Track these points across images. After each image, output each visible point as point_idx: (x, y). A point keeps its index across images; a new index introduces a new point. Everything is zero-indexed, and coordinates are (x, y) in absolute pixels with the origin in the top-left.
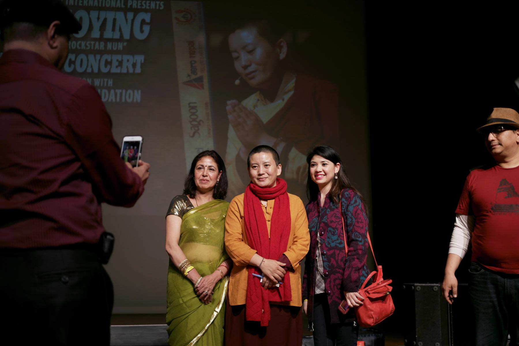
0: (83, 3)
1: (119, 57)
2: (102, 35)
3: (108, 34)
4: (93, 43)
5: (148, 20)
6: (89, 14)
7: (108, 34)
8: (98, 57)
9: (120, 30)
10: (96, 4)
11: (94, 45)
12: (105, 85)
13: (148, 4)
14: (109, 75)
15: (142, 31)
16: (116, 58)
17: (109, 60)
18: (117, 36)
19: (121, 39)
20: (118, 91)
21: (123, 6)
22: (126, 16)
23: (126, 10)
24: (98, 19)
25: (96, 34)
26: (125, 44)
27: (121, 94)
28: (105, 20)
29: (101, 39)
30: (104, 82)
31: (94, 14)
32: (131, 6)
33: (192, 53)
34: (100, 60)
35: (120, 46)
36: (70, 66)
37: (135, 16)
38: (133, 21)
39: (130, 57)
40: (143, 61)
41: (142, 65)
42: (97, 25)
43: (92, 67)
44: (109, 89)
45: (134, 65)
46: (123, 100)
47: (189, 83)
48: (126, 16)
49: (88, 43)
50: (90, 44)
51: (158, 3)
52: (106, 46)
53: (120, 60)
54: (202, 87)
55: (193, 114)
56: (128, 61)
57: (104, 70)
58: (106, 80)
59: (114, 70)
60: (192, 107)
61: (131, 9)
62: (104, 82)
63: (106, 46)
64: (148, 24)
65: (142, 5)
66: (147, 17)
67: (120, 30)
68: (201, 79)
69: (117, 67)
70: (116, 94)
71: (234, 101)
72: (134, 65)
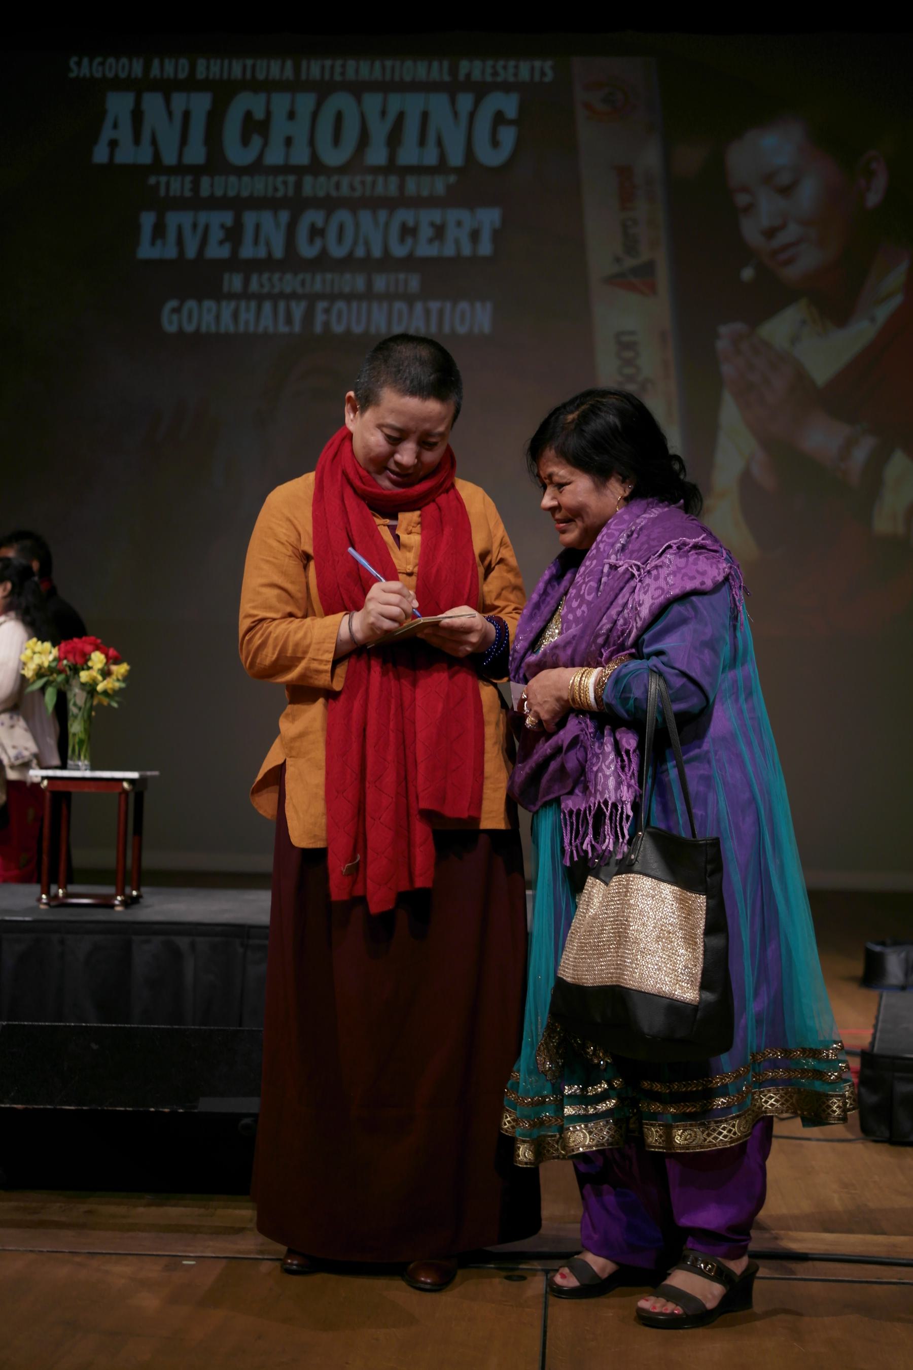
0: (343, 74)
1: (436, 215)
2: (392, 157)
3: (408, 155)
4: (369, 179)
5: (511, 112)
6: (359, 101)
7: (408, 155)
8: (383, 215)
9: (440, 143)
10: (377, 74)
11: (374, 183)
13: (511, 70)
14: (410, 263)
15: (495, 143)
16: (428, 217)
17: (411, 223)
18: (431, 158)
19: (442, 167)
20: (434, 306)
21: (447, 78)
22: (453, 102)
23: (452, 89)
24: (383, 113)
25: (377, 155)
26: (452, 179)
27: (441, 313)
28: (401, 116)
29: (390, 167)
31: (372, 102)
32: (468, 75)
33: (626, 198)
34: (387, 225)
35: (440, 185)
36: (311, 240)
37: (477, 103)
38: (472, 115)
39: (464, 215)
40: (497, 224)
41: (497, 235)
42: (379, 131)
43: (367, 243)
44: (410, 299)
45: (475, 236)
46: (447, 329)
47: (618, 280)
48: (453, 102)
49: (358, 179)
50: (363, 183)
51: (537, 64)
52: (402, 187)
53: (438, 221)
54: (652, 289)
55: (629, 362)
56: (459, 224)
57: (399, 251)
58: (402, 276)
59: (425, 250)
60: (626, 345)
61: (469, 85)
63: (402, 187)
64: (511, 122)
65: (495, 74)
66: (509, 105)
67: (440, 143)
68: (647, 269)
69: (431, 241)
71: (739, 327)
72: (475, 236)
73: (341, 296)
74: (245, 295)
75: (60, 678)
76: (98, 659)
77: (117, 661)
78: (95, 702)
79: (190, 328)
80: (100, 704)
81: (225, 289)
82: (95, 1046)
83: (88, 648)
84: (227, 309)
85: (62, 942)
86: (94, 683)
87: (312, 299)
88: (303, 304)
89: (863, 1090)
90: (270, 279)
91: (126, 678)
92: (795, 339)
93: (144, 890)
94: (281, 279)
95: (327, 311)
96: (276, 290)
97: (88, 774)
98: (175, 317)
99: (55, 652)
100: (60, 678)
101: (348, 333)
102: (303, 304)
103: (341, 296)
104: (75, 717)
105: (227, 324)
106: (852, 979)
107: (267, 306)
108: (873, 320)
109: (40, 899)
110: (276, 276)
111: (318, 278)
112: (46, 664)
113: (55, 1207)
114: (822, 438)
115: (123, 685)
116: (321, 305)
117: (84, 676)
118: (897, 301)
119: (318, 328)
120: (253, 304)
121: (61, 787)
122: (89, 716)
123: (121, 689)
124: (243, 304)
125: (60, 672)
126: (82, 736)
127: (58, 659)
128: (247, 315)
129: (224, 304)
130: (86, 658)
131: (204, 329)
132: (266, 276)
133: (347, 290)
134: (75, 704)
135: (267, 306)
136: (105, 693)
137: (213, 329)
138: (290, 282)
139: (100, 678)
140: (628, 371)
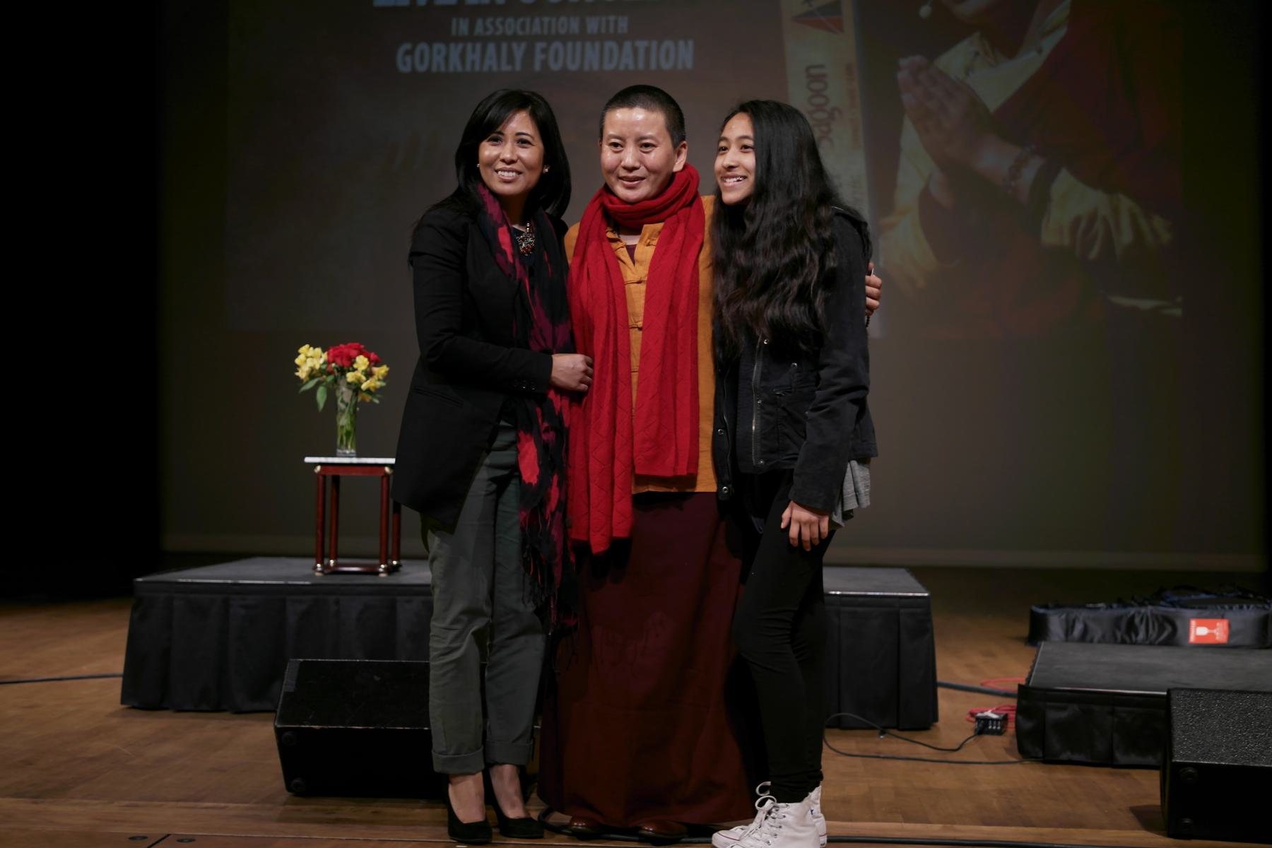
12: (612, 31)
20: (641, 44)
27: (648, 50)
30: (608, 22)
44: (620, 39)
46: (653, 66)
55: (817, 93)
58: (612, 18)
60: (815, 77)
62: (608, 22)
68: (834, 9)
70: (635, 51)
71: (917, 59)
73: (558, 37)
74: (471, 38)
75: (330, 378)
76: (362, 362)
77: (377, 363)
78: (360, 399)
79: (421, 68)
80: (363, 401)
81: (454, 32)
82: (377, 678)
83: (353, 352)
84: (455, 50)
85: (337, 602)
86: (359, 382)
87: (532, 40)
88: (523, 45)
89: (1020, 718)
90: (493, 23)
91: (386, 378)
92: (969, 70)
93: (403, 562)
94: (503, 23)
95: (545, 51)
96: (499, 33)
97: (355, 460)
98: (408, 59)
99: (325, 356)
100: (330, 378)
101: (564, 70)
102: (523, 45)
103: (558, 37)
104: (343, 412)
105: (455, 64)
106: (1019, 639)
107: (491, 48)
108: (1040, 51)
109: (315, 568)
110: (499, 20)
111: (537, 21)
112: (317, 367)
113: (348, 809)
114: (994, 159)
115: (384, 384)
116: (540, 46)
117: (350, 377)
118: (1062, 33)
119: (537, 67)
120: (478, 46)
121: (331, 472)
122: (355, 411)
123: (381, 388)
124: (469, 46)
125: (330, 373)
126: (349, 428)
127: (327, 363)
128: (473, 55)
129: (452, 46)
130: (352, 361)
131: (434, 69)
132: (489, 20)
133: (562, 31)
134: (342, 401)
135: (491, 48)
136: (368, 391)
137: (443, 69)
138: (511, 25)
139: (364, 378)
140: (818, 100)
